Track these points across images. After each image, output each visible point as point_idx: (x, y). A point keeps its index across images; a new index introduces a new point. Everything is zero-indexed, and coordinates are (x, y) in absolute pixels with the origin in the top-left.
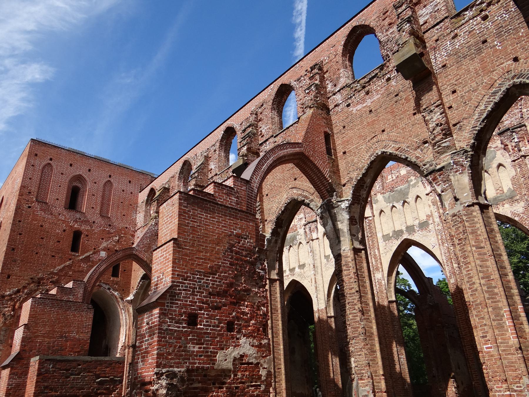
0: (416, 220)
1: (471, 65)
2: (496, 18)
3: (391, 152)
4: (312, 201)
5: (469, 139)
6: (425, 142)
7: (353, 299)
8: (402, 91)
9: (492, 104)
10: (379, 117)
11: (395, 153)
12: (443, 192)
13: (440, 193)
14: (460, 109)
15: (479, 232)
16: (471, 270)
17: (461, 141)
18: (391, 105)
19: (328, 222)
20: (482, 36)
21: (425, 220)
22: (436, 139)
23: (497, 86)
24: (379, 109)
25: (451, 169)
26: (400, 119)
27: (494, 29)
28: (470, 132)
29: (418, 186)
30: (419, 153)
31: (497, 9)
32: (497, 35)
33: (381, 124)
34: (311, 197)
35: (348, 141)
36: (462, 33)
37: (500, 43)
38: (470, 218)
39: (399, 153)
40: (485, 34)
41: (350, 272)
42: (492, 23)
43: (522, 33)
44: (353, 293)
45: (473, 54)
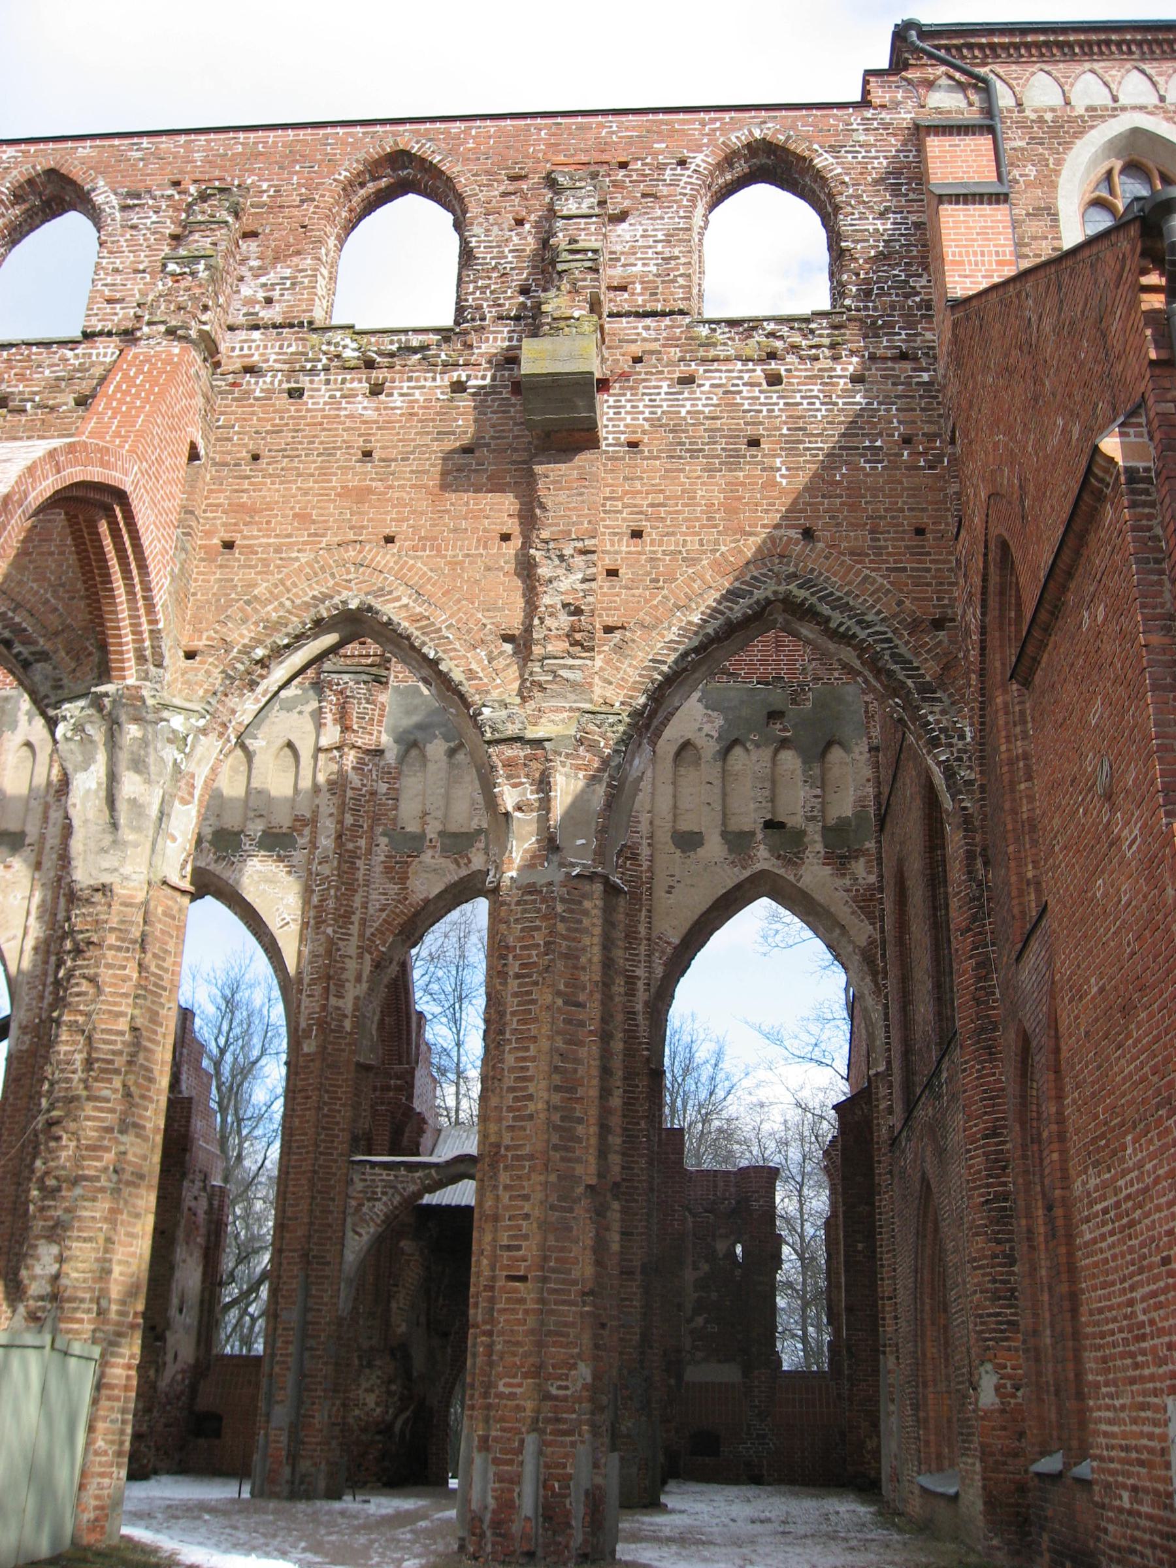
0: (258, 821)
1: (704, 484)
2: (798, 400)
3: (395, 619)
5: (634, 689)
7: (114, 1053)
8: (488, 445)
10: (390, 487)
11: (406, 629)
12: (519, 808)
13: (510, 809)
14: (636, 592)
15: (583, 960)
16: (533, 1059)
17: (610, 683)
20: (754, 424)
21: (284, 830)
22: (550, 648)
24: (395, 460)
26: (455, 530)
27: (785, 423)
28: (643, 669)
29: (300, 713)
31: (806, 377)
32: (787, 442)
33: (387, 513)
34: (41, 641)
35: (252, 511)
36: (708, 383)
37: (788, 469)
40: (761, 423)
42: (786, 404)
43: (843, 475)
45: (718, 456)
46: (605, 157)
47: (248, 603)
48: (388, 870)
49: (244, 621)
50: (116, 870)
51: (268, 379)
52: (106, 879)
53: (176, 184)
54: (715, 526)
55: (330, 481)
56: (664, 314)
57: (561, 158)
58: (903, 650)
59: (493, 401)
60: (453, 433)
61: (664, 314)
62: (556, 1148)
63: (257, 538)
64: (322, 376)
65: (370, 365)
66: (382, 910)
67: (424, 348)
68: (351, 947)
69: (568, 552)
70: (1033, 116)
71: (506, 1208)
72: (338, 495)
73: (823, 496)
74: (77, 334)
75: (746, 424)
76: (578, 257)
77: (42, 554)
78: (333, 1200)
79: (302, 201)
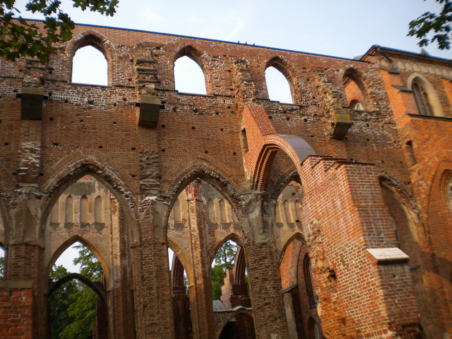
4: (229, 182)
7: (278, 285)
19: (254, 211)
44: (277, 280)
48: (210, 233)
50: (265, 239)
52: (264, 241)
53: (225, 56)
57: (313, 65)
64: (275, 114)
65: (285, 112)
66: (210, 244)
67: (296, 109)
77: (220, 154)
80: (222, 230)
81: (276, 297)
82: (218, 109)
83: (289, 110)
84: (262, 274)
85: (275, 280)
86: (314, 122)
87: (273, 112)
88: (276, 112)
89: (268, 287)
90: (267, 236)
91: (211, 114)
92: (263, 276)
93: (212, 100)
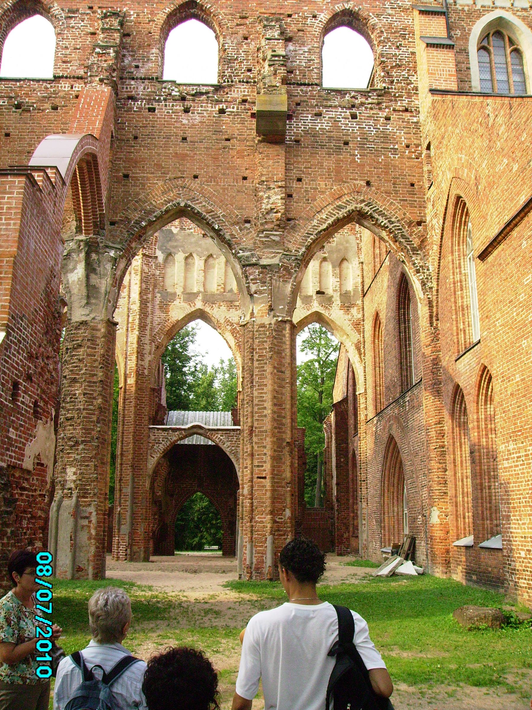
1: (326, 160)
5: (300, 245)
6: (248, 221)
9: (335, 218)
10: (195, 154)
11: (205, 216)
12: (256, 293)
14: (300, 204)
15: (283, 354)
16: (266, 393)
18: (216, 147)
19: (75, 268)
20: (346, 135)
22: (266, 227)
23: (345, 201)
25: (276, 272)
26: (224, 174)
30: (237, 231)
33: (194, 165)
35: (136, 162)
36: (327, 116)
38: (279, 335)
39: (210, 218)
40: (349, 135)
41: (95, 352)
43: (382, 160)
44: (94, 382)
45: (332, 149)
46: (282, 11)
47: (137, 202)
48: (161, 308)
49: (135, 210)
51: (139, 103)
52: (84, 318)
53: (91, 8)
54: (331, 178)
55: (169, 150)
56: (309, 85)
57: (263, 10)
58: (405, 234)
59: (238, 118)
60: (221, 132)
61: (309, 85)
62: (275, 428)
63: (139, 173)
64: (163, 103)
65: (183, 99)
66: (159, 325)
67: (207, 93)
68: (147, 340)
69: (272, 186)
70: (460, 8)
71: (256, 451)
72: (173, 156)
73: (375, 168)
74: (50, 76)
75: (343, 135)
76: (276, 59)
78: (142, 443)
79: (149, 21)
80: (183, 304)
81: (84, 409)
82: (57, 102)
83: (193, 95)
84: (71, 371)
85: (90, 382)
86: (238, 114)
87: (159, 99)
88: (165, 100)
89: (77, 392)
90: (91, 311)
91: (43, 110)
92: (73, 374)
93: (49, 86)
